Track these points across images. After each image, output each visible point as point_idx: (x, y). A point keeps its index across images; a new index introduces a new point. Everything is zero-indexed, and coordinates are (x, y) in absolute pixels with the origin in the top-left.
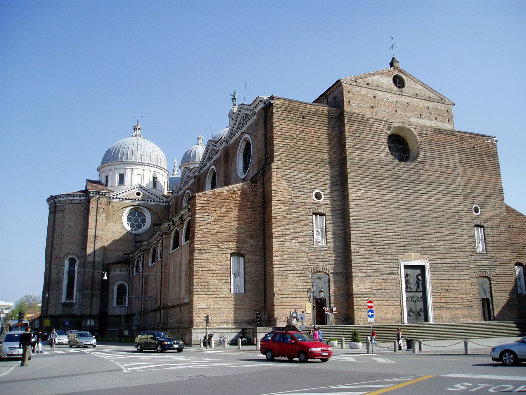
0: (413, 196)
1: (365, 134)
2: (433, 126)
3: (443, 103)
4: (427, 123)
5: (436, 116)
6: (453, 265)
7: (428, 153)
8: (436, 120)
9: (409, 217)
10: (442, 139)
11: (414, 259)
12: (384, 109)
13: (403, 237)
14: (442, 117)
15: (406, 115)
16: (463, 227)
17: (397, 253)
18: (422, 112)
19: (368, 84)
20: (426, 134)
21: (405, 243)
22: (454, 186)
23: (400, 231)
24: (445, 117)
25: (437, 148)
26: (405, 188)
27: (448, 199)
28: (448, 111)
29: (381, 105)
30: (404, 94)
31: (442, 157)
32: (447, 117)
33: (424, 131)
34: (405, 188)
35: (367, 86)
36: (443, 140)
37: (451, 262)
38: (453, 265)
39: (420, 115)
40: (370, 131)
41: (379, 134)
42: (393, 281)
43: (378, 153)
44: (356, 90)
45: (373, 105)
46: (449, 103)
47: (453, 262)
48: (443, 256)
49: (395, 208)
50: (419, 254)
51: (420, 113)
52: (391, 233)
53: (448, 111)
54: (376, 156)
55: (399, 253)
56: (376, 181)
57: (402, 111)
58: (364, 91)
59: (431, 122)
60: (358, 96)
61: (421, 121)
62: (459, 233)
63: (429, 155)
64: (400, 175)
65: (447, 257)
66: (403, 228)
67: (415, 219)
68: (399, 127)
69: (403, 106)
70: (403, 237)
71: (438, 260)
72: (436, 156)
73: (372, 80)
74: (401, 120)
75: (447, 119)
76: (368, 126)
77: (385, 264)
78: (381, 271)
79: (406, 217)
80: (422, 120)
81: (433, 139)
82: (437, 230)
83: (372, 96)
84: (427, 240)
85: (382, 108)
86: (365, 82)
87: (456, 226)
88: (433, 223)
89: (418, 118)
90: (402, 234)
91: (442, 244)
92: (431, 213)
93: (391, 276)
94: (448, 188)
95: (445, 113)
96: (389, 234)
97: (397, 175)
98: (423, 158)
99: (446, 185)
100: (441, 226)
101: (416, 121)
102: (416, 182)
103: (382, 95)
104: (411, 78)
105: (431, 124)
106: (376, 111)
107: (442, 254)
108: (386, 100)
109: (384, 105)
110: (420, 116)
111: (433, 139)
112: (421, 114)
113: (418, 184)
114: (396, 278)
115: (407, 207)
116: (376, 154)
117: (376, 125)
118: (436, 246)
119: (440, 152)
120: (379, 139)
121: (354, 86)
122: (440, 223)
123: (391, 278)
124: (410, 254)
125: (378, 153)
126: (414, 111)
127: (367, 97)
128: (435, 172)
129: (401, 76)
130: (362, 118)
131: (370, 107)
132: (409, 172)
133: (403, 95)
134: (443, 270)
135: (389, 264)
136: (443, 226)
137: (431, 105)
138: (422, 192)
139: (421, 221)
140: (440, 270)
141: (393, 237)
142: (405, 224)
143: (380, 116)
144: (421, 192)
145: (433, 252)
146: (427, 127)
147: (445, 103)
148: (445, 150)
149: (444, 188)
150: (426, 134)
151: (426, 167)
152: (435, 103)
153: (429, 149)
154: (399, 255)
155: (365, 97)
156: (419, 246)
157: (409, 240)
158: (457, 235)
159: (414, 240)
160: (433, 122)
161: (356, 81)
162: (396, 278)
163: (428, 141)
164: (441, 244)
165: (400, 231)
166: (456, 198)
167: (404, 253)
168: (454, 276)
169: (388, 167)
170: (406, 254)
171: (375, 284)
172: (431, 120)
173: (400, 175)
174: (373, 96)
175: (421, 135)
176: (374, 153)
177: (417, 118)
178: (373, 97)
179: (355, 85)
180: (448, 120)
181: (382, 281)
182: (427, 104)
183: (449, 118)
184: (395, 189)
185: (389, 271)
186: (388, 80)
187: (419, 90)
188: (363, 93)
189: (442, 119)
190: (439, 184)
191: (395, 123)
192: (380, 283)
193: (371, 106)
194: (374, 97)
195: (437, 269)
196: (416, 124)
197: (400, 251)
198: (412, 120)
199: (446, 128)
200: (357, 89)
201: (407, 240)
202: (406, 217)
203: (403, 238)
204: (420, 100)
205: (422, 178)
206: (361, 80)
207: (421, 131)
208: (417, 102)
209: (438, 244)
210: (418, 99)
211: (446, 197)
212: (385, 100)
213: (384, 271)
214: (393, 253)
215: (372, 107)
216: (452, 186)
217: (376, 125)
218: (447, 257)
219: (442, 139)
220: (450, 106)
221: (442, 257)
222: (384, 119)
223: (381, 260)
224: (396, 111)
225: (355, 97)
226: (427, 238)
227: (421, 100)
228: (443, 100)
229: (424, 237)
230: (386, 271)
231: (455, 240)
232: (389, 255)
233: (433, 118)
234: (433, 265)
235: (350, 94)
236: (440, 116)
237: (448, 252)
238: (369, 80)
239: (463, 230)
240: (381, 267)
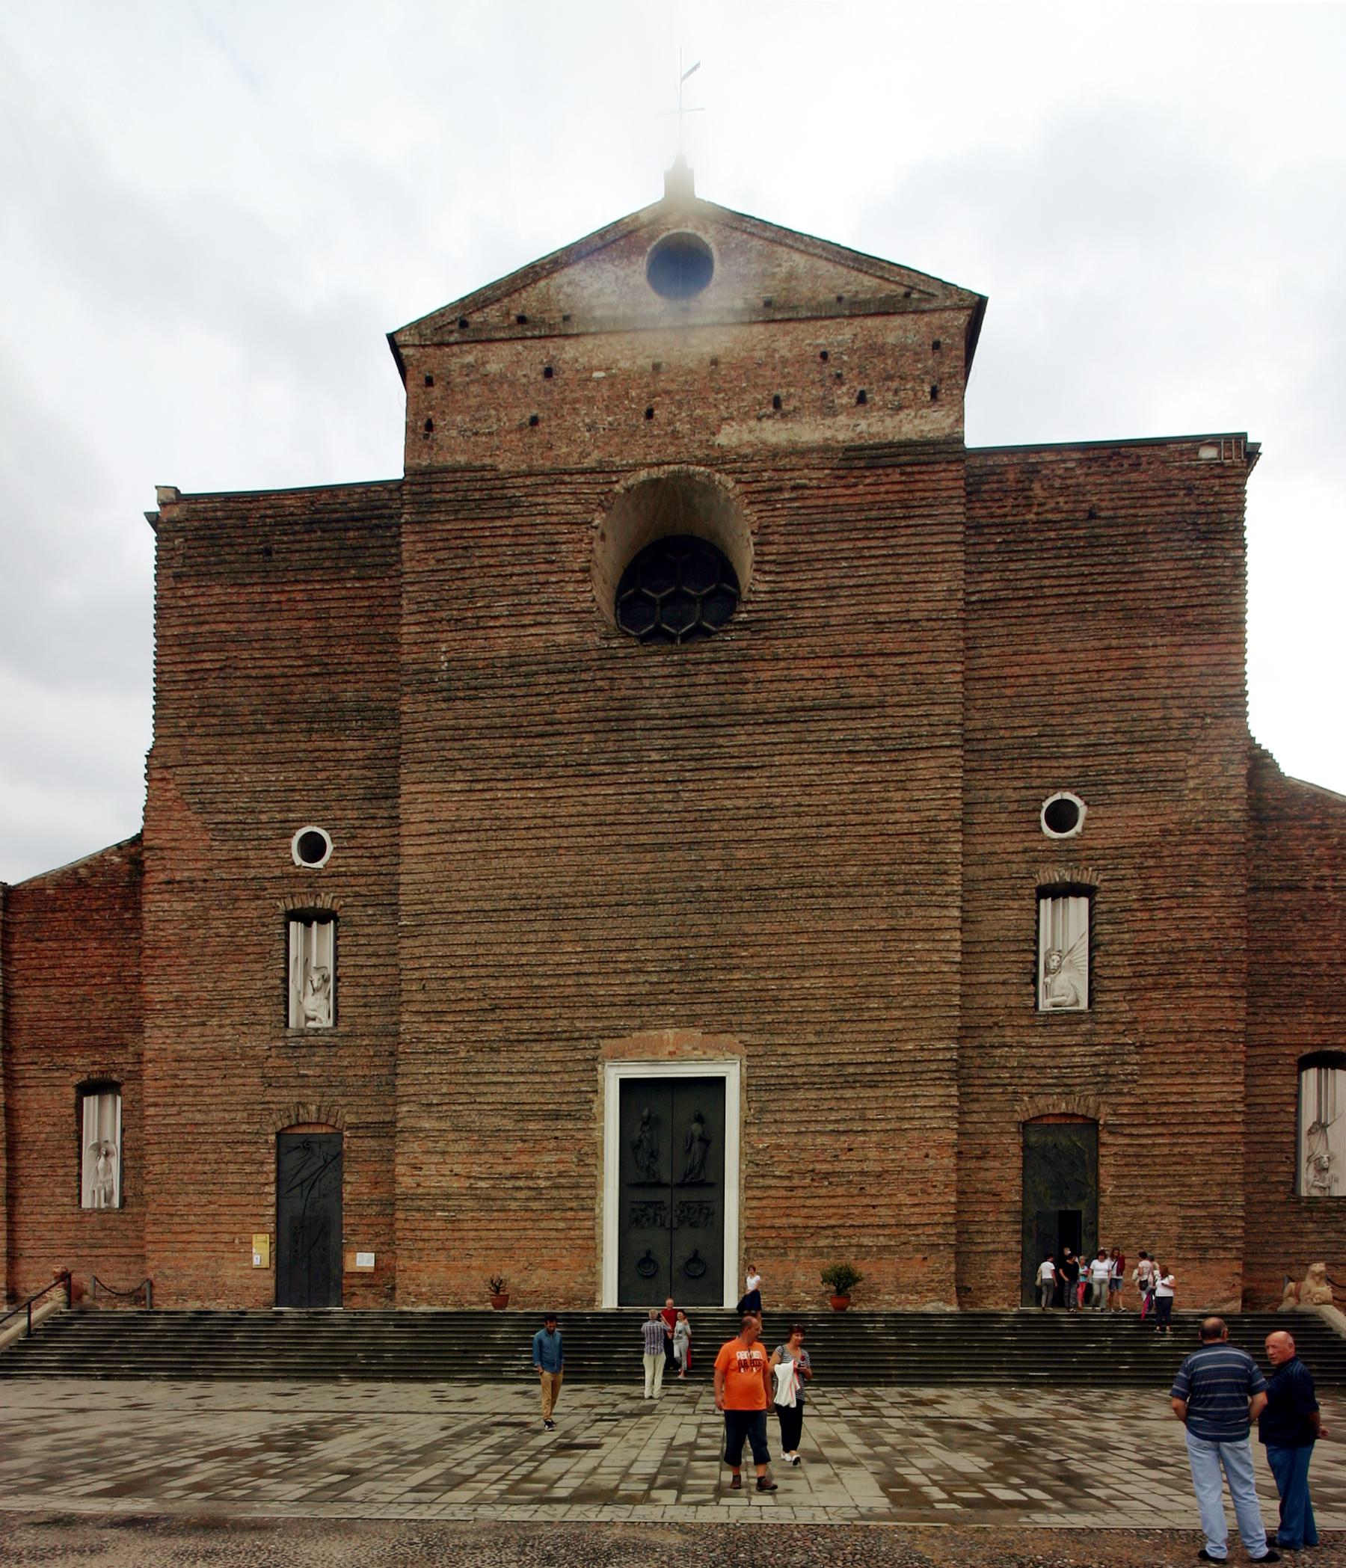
0: (691, 786)
1: (487, 551)
2: (841, 438)
3: (914, 312)
4: (809, 432)
5: (860, 388)
6: (869, 1069)
7: (795, 576)
8: (860, 408)
9: (664, 880)
10: (887, 493)
11: (671, 1053)
12: (587, 420)
13: (629, 966)
14: (894, 385)
15: (700, 419)
16: (947, 895)
17: (595, 1034)
18: (789, 385)
19: (522, 320)
20: (794, 488)
21: (634, 990)
22: (921, 710)
23: (613, 945)
24: (915, 379)
25: (845, 545)
26: (655, 756)
27: (879, 776)
28: (936, 345)
29: (576, 401)
30: (699, 321)
31: (870, 580)
32: (927, 378)
33: (788, 475)
34: (655, 756)
35: (518, 331)
36: (892, 497)
37: (860, 1058)
38: (869, 1069)
39: (777, 402)
40: (510, 531)
41: (556, 538)
42: (567, 1144)
43: (541, 624)
44: (462, 366)
45: (535, 412)
46: (948, 303)
47: (870, 1058)
48: (817, 1033)
49: (601, 849)
50: (697, 1033)
51: (775, 392)
52: (576, 953)
53: (936, 345)
54: (533, 640)
55: (606, 1033)
56: (522, 746)
57: (680, 405)
58: (498, 359)
59: (828, 422)
60: (474, 389)
61: (775, 433)
62: (923, 924)
63: (798, 585)
64: (638, 703)
65: (838, 1037)
66: (633, 931)
67: (692, 886)
68: (656, 482)
69: (686, 382)
70: (629, 966)
71: (794, 1050)
72: (837, 582)
73: (545, 299)
74: (672, 449)
75: (927, 389)
76: (505, 513)
77: (537, 1079)
78: (516, 1107)
79: (647, 881)
80: (781, 425)
81: (831, 502)
82: (804, 920)
83: (536, 375)
84: (748, 969)
85: (585, 414)
86: (508, 314)
87: (905, 893)
88: (785, 894)
89: (759, 419)
90: (622, 957)
91: (822, 982)
92: (780, 850)
93: (560, 1124)
94: (887, 722)
95: (918, 361)
96: (565, 959)
97: (625, 703)
98: (768, 606)
99: (873, 713)
100: (821, 901)
101: (746, 437)
102: (719, 721)
103: (583, 355)
104: (744, 231)
105: (828, 434)
106: (550, 434)
107: (818, 1028)
108: (602, 374)
109: (590, 401)
110: (771, 409)
111: (831, 502)
112: (782, 392)
113: (722, 731)
114: (580, 1135)
115: (661, 839)
116: (533, 631)
117: (541, 500)
118: (787, 994)
119: (864, 557)
120: (552, 562)
121: (456, 349)
122: (819, 892)
123: (558, 1134)
124: (652, 1033)
125: (541, 624)
126: (744, 390)
127: (512, 384)
128: (824, 663)
129: (693, 235)
130: (478, 485)
131: (520, 428)
132: (685, 681)
133: (693, 327)
134: (813, 1095)
135: (557, 1078)
136: (834, 903)
137: (841, 335)
138: (743, 762)
139: (722, 890)
140: (800, 1095)
141: (587, 969)
142: (642, 911)
143: (569, 454)
144: (734, 763)
145: (769, 1018)
146: (803, 452)
147: (925, 306)
148: (892, 541)
149: (865, 728)
150: (794, 488)
151: (780, 647)
152: (869, 322)
153: (803, 557)
154: (602, 1042)
155: (501, 384)
156: (705, 998)
157: (654, 978)
158: (905, 935)
159: (679, 977)
160: (842, 419)
161: (464, 324)
162: (580, 1135)
163: (802, 520)
164: (815, 981)
165: (613, 945)
166: (926, 767)
167: (625, 1033)
168: (870, 1115)
169: (584, 676)
170: (636, 1034)
171: (485, 1157)
172: (829, 410)
173: (638, 703)
174: (541, 368)
175: (763, 496)
176: (523, 626)
177: (752, 423)
178: (540, 377)
179: (457, 343)
180: (934, 393)
181: (520, 1145)
182: (817, 337)
183: (941, 380)
184: (607, 769)
185: (551, 1107)
186: (622, 274)
187: (781, 281)
188: (493, 368)
189: (896, 392)
190: (834, 714)
191: (634, 468)
192: (509, 1155)
193: (526, 420)
194: (548, 373)
195: (783, 1089)
196: (748, 451)
197: (607, 1023)
198: (728, 437)
199: (915, 438)
200: (470, 359)
201: (642, 978)
202: (647, 881)
203: (627, 972)
204: (781, 326)
205: (749, 701)
206: (493, 314)
207: (770, 479)
208: (765, 344)
209: (796, 984)
210: (772, 326)
211: (867, 767)
212: (597, 375)
213: (527, 1107)
214: (576, 1035)
215: (534, 421)
216: (909, 711)
217: (541, 500)
218: (838, 1037)
219: (887, 493)
220: (952, 314)
221: (812, 1039)
222: (588, 463)
223: (520, 1066)
224: (650, 414)
225: (459, 397)
226: (747, 962)
227: (790, 326)
228: (915, 295)
229: (730, 956)
230: (536, 1107)
231: (895, 957)
232: (555, 1046)
233: (845, 400)
234: (759, 1072)
235: (437, 391)
236: (890, 378)
237: (847, 1016)
238: (527, 301)
239: (945, 912)
240: (520, 1093)
